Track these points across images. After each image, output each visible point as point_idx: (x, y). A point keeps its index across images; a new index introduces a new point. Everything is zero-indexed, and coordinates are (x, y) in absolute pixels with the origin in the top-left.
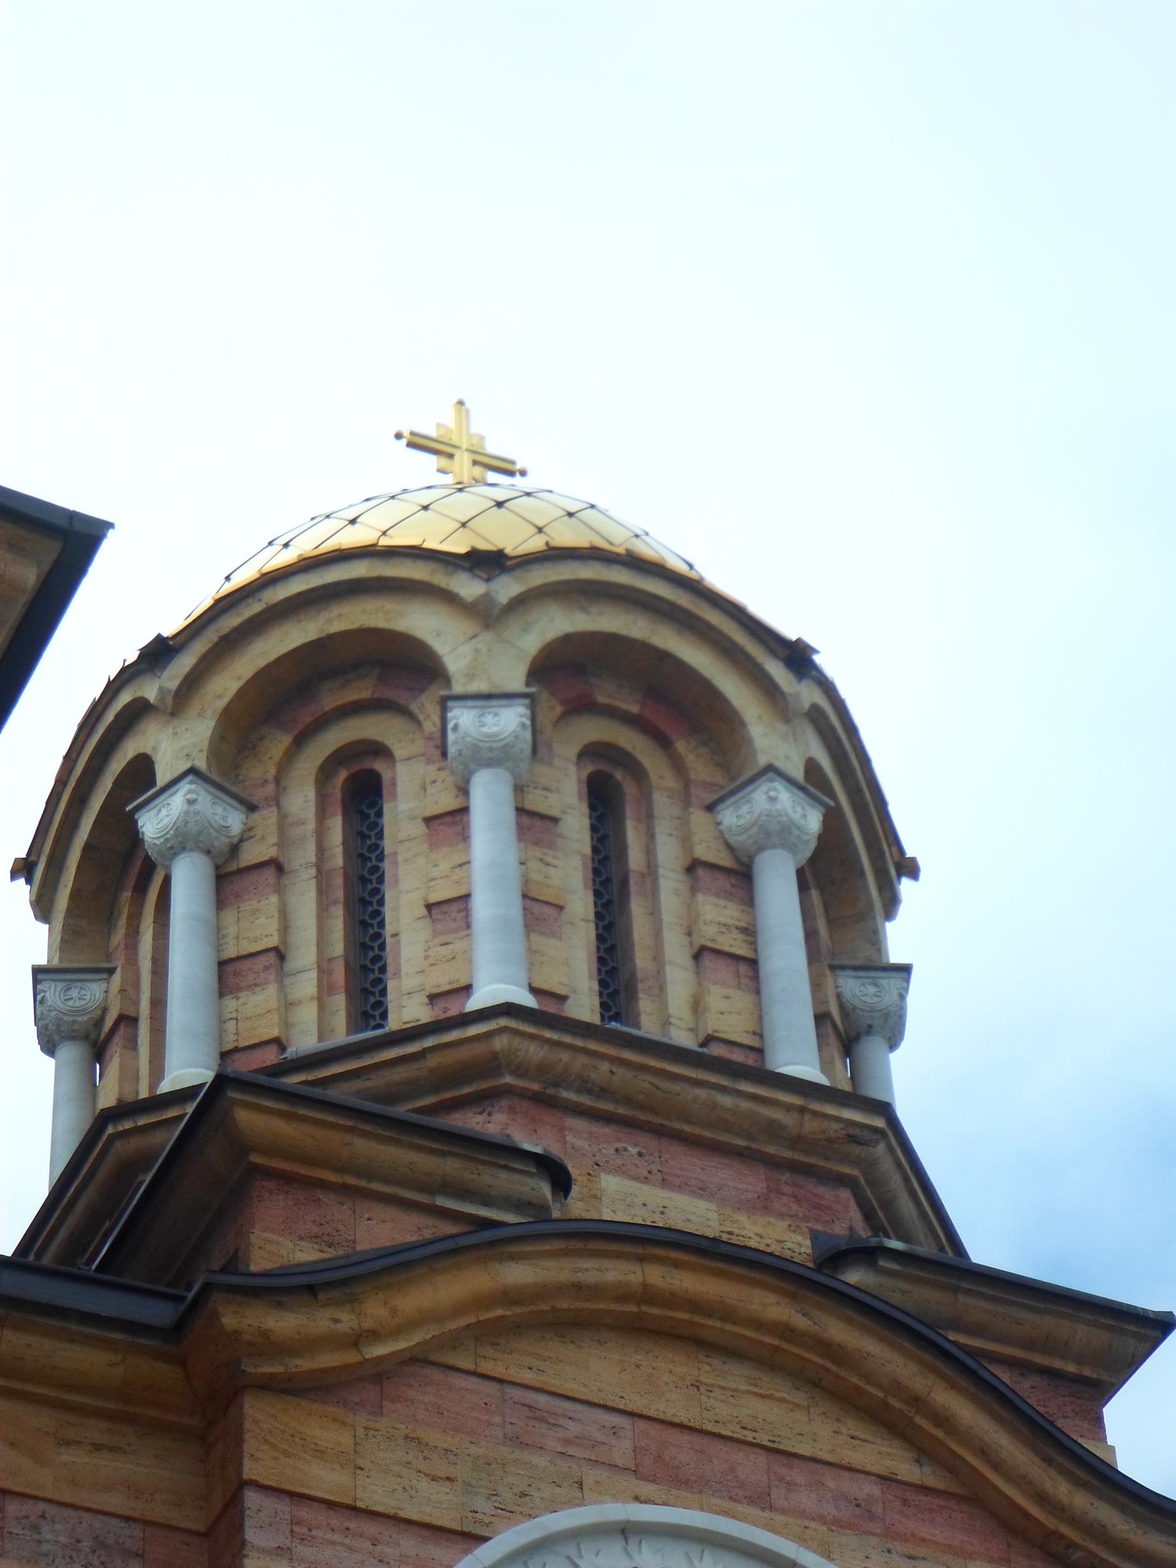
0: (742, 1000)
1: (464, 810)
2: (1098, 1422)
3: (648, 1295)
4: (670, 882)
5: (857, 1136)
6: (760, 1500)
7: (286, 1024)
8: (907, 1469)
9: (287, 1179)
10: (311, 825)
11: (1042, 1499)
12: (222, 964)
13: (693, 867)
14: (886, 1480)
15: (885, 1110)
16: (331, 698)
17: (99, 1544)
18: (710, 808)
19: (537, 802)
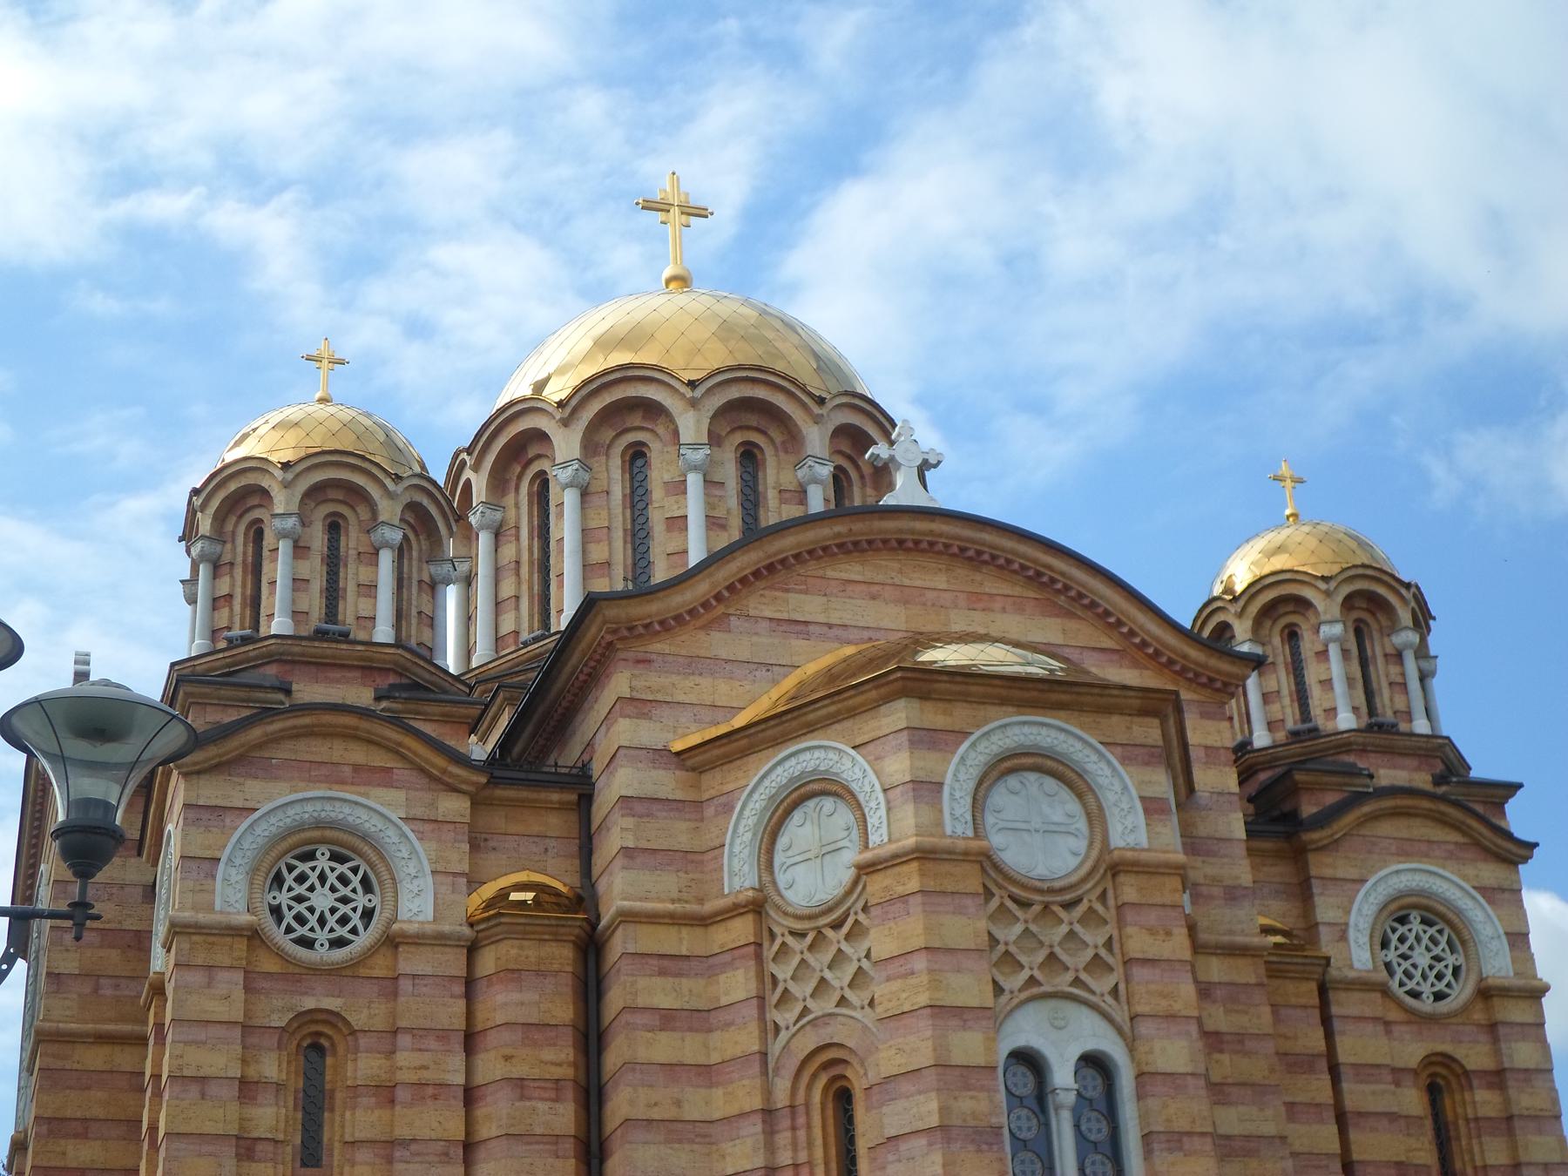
0: (1403, 698)
1: (1327, 651)
2: (1503, 813)
3: (1396, 807)
4: (1380, 661)
5: (1441, 746)
6: (1427, 856)
7: (1284, 714)
8: (1459, 838)
9: (1307, 789)
10: (1281, 649)
11: (1495, 845)
12: (1263, 694)
13: (1386, 655)
14: (1456, 843)
15: (1448, 738)
16: (1282, 610)
17: (1276, 892)
18: (1389, 635)
19: (1345, 647)
